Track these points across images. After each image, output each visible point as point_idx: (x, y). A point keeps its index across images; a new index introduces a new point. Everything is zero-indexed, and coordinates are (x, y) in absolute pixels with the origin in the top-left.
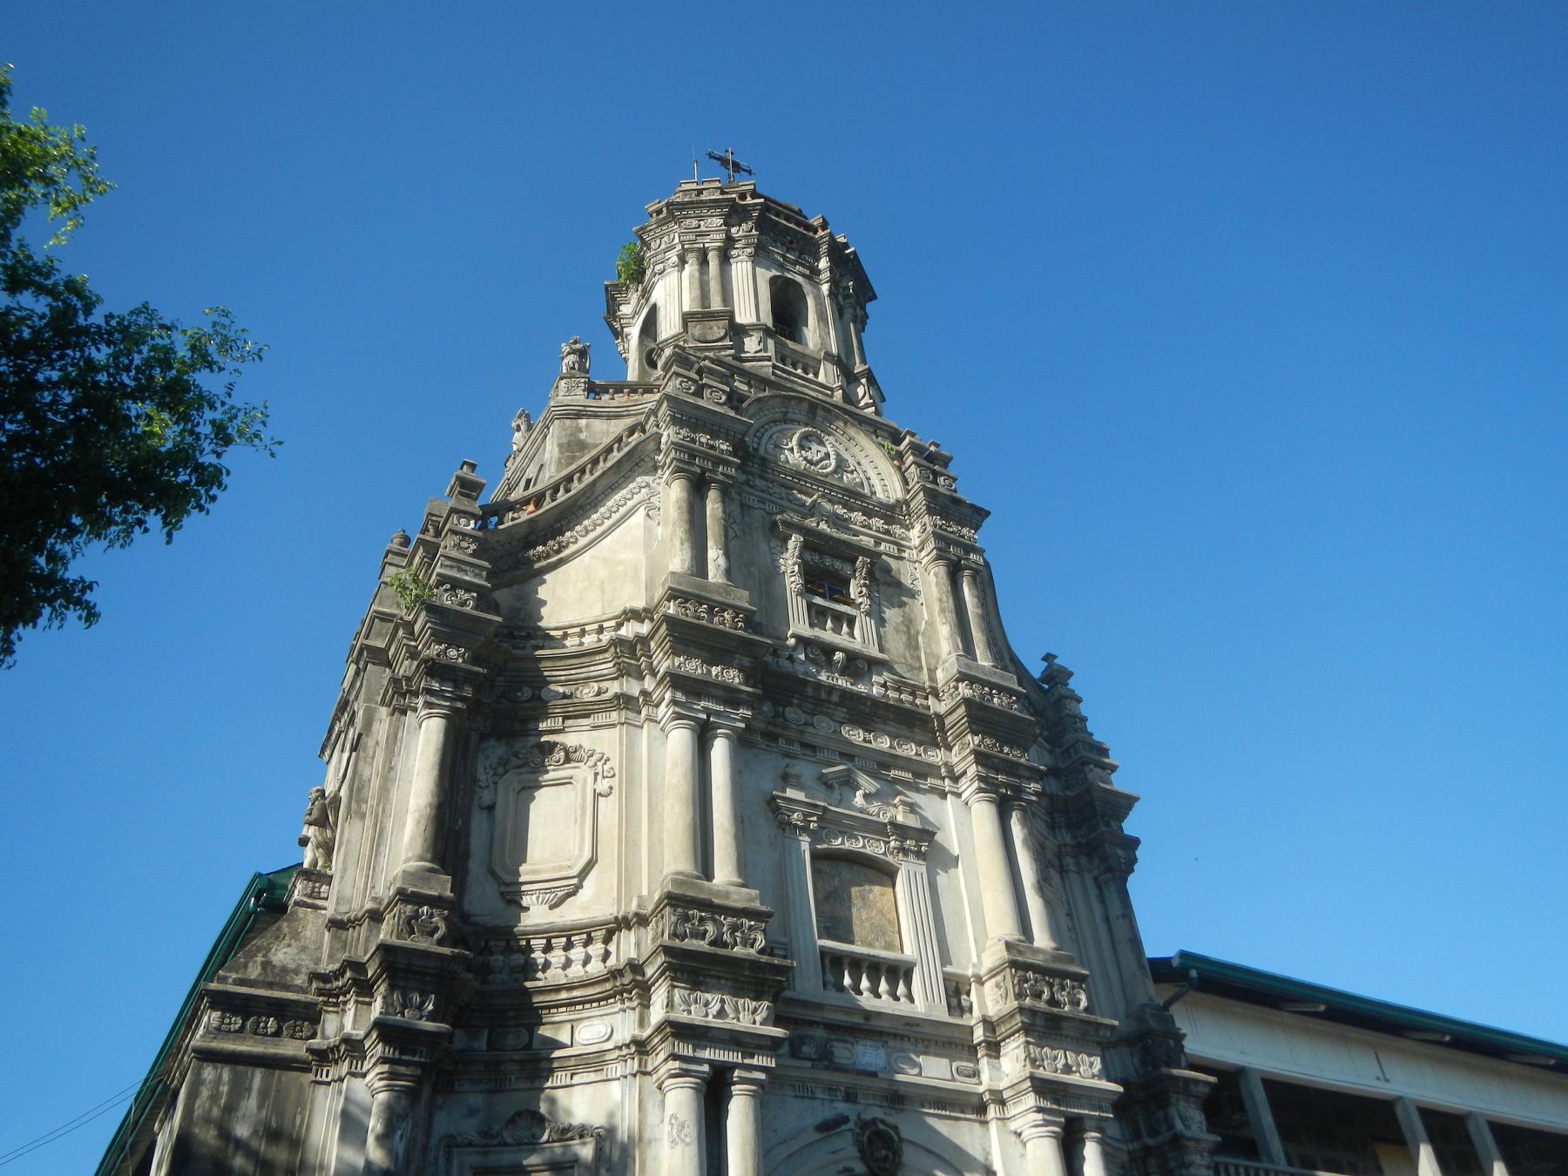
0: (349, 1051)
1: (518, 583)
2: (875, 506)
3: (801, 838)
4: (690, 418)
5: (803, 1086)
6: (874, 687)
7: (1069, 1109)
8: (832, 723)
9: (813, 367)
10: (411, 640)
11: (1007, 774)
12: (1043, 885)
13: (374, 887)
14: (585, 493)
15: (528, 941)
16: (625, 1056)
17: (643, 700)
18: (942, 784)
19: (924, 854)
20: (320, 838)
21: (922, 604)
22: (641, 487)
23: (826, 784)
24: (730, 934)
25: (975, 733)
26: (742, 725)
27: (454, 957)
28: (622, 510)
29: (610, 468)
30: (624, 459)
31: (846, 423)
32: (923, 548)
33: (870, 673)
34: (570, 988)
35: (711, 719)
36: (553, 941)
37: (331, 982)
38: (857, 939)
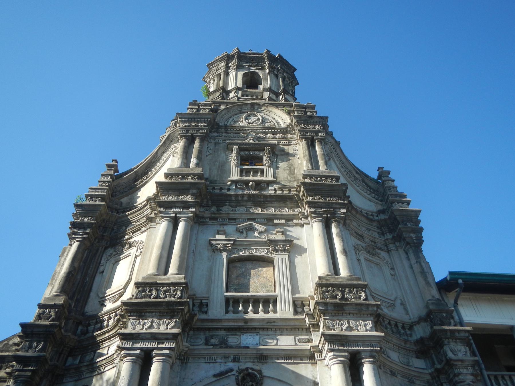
1: (131, 194)
2: (278, 130)
3: (223, 254)
4: (188, 119)
5: (210, 357)
6: (271, 191)
7: (350, 348)
8: (245, 209)
9: (260, 95)
11: (327, 208)
12: (345, 252)
14: (154, 157)
15: (103, 317)
18: (301, 221)
19: (288, 250)
22: (173, 148)
23: (240, 231)
24: (164, 294)
26: (192, 215)
27: (51, 326)
30: (167, 140)
31: (267, 106)
33: (268, 186)
35: (177, 215)
36: (111, 315)
38: (251, 291)
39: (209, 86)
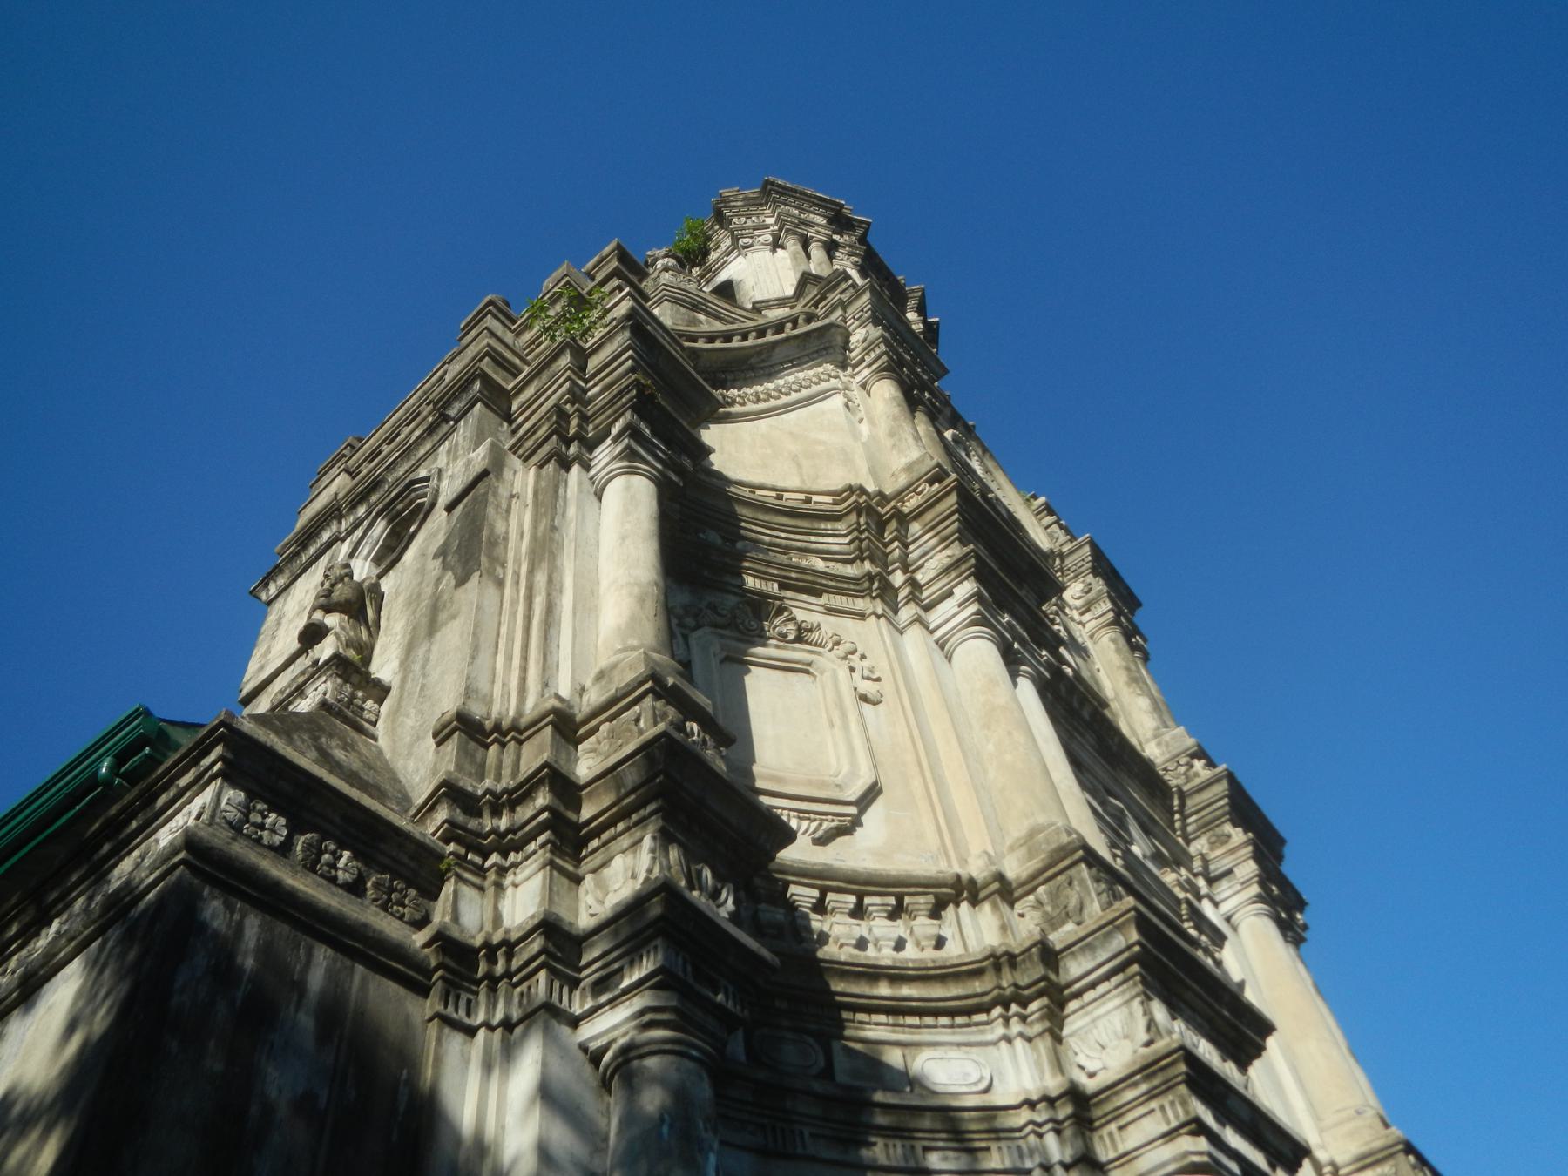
0: (550, 955)
10: (580, 378)
13: (546, 685)
14: (759, 353)
16: (1040, 1125)
17: (911, 593)
20: (352, 634)
21: (1099, 670)
25: (1235, 825)
28: (805, 393)
29: (796, 337)
30: (815, 334)
32: (1088, 610)
34: (897, 976)
36: (830, 896)
37: (479, 815)
39: (749, 241)
